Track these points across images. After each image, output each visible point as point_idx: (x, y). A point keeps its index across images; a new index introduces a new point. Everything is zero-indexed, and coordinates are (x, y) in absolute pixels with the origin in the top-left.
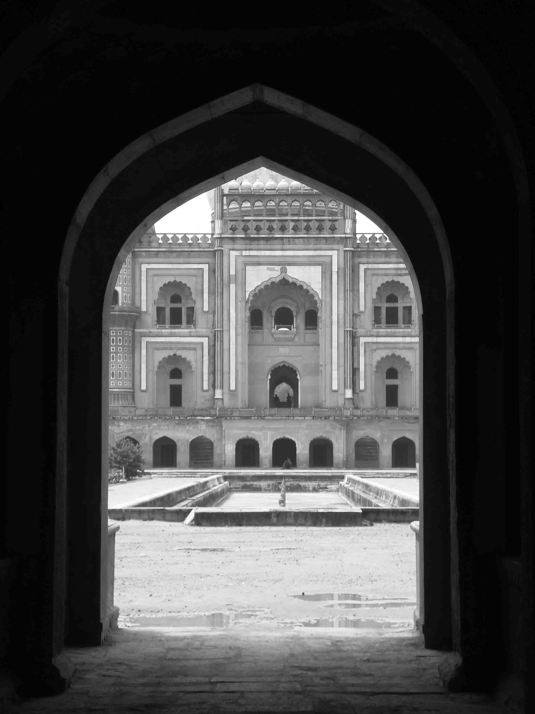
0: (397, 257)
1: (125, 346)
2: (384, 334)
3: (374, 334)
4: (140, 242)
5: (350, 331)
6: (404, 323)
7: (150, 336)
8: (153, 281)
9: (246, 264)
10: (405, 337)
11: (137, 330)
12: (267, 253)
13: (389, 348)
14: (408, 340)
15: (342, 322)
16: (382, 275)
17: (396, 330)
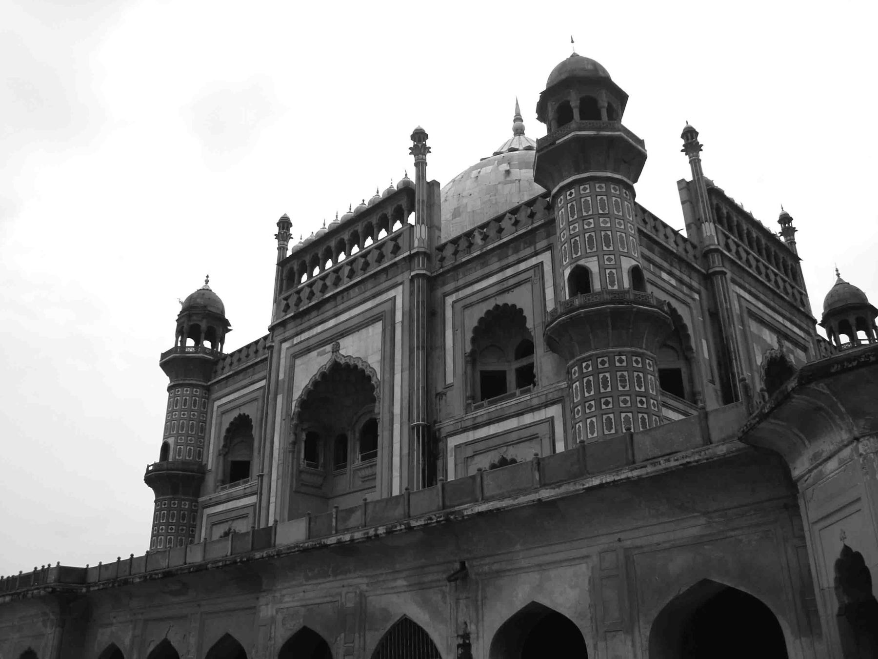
0: (500, 260)
1: (171, 524)
2: (485, 418)
3: (469, 423)
4: (216, 372)
5: (418, 426)
6: (519, 385)
7: (210, 506)
8: (221, 423)
9: (295, 356)
10: (522, 414)
11: (200, 500)
12: (319, 329)
13: (496, 447)
14: (528, 419)
15: (406, 412)
16: (479, 302)
17: (505, 404)
